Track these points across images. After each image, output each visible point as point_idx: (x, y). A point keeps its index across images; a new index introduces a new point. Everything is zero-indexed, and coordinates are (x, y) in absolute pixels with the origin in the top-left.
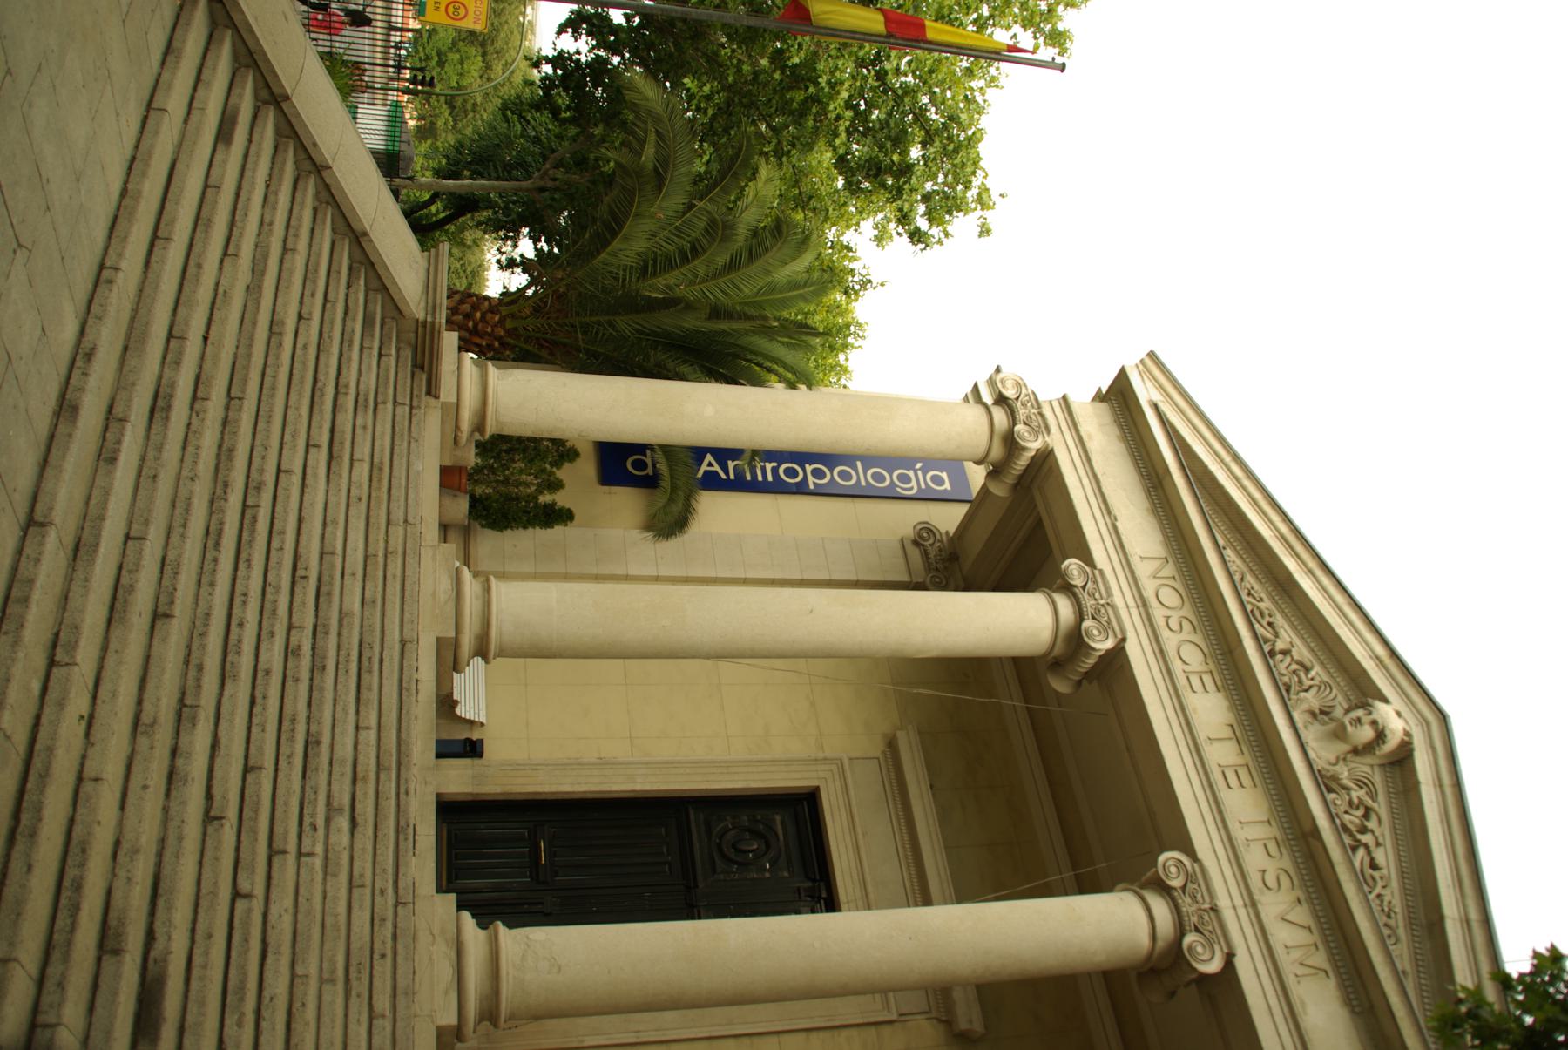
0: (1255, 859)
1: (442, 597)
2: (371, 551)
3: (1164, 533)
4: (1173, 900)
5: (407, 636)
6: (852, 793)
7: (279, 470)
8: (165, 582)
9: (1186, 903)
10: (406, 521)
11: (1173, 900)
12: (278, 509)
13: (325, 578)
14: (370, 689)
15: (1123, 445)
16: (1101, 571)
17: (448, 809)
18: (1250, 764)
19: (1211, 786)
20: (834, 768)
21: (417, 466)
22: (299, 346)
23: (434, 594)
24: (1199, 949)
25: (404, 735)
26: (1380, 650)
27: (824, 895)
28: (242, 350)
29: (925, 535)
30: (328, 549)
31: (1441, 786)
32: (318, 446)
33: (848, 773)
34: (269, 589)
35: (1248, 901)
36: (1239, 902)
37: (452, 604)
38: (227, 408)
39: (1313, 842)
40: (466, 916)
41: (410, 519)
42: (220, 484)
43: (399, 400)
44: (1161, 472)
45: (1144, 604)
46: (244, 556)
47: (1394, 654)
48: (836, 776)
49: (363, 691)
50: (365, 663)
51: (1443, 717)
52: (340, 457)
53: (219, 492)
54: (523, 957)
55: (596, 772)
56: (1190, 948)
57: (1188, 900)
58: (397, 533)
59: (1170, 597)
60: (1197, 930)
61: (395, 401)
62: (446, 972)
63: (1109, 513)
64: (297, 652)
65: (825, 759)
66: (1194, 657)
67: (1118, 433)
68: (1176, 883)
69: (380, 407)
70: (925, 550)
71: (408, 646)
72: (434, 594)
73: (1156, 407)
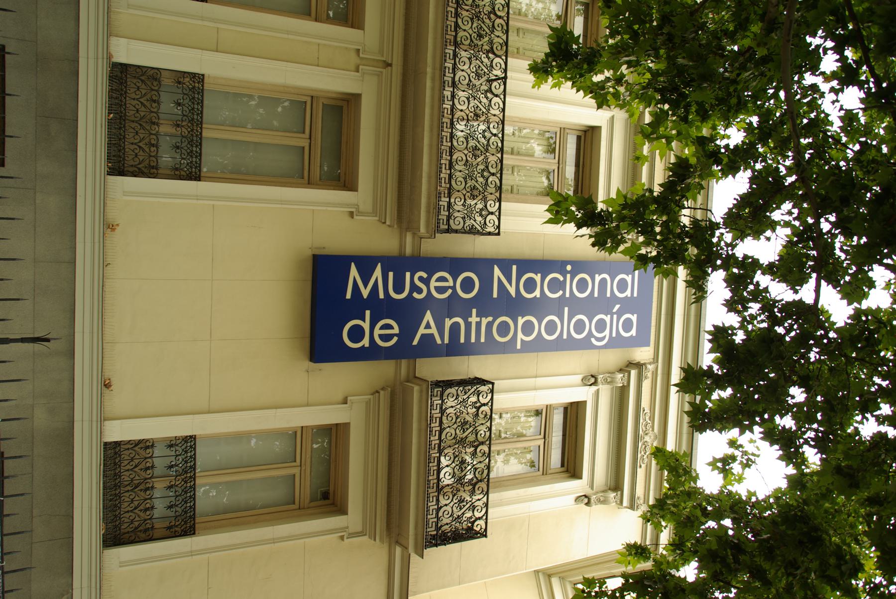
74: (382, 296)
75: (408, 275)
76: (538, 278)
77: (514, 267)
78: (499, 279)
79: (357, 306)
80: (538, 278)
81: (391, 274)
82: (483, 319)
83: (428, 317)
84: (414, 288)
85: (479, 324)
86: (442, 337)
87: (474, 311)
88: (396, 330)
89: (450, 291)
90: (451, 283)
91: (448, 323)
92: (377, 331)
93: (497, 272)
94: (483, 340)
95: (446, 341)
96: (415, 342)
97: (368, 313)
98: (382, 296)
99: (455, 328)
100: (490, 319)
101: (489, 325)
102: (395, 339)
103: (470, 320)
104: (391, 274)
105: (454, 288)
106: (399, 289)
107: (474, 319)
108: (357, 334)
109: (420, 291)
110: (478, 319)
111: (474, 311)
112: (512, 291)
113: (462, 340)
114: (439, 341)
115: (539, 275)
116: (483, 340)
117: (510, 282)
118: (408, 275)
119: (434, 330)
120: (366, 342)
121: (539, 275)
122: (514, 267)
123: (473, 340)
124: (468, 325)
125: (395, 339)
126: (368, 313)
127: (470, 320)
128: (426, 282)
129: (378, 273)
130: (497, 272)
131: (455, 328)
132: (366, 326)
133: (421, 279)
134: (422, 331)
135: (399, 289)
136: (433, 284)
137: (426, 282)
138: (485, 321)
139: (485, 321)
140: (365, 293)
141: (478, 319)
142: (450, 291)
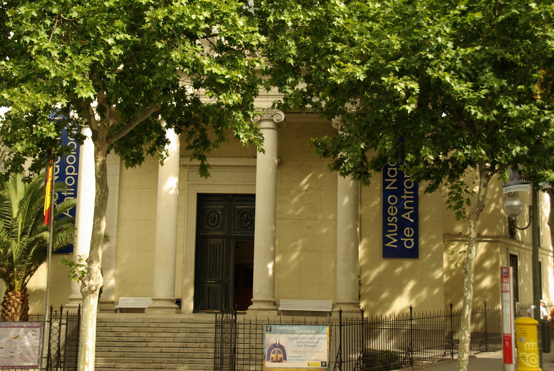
1: (163, 312)
2: (163, 331)
4: (263, 120)
5: (179, 321)
6: (200, 183)
7: (161, 352)
8: (209, 368)
9: (265, 117)
10: (143, 322)
11: (263, 120)
12: (172, 351)
13: (181, 341)
14: (203, 330)
17: (196, 310)
20: (191, 187)
21: (123, 320)
22: (120, 351)
23: (163, 314)
24: (278, 118)
25: (208, 322)
27: (231, 197)
28: (138, 362)
30: (173, 341)
32: (147, 345)
33: (193, 183)
34: (194, 352)
35: (266, 97)
36: (266, 99)
37: (165, 310)
38: (156, 363)
40: (249, 308)
41: (142, 321)
42: (178, 362)
43: (104, 325)
46: (191, 357)
48: (194, 187)
49: (203, 332)
50: (196, 331)
52: (144, 339)
53: (180, 362)
54: (262, 295)
55: (188, 264)
56: (277, 120)
57: (264, 116)
58: (151, 325)
60: (272, 116)
61: (104, 327)
62: (265, 313)
64: (206, 346)
65: (188, 189)
69: (113, 330)
71: (183, 321)
72: (163, 314)
74: (396, 234)
75: (389, 224)
76: (390, 169)
77: (386, 180)
78: (390, 187)
79: (400, 243)
80: (390, 169)
81: (389, 231)
82: (405, 193)
83: (403, 216)
84: (393, 222)
85: (407, 195)
86: (411, 210)
87: (402, 197)
88: (408, 228)
89: (395, 207)
90: (392, 207)
91: (406, 208)
92: (408, 236)
93: (388, 188)
94: (412, 193)
95: (413, 208)
96: (412, 221)
97: (402, 239)
98: (396, 234)
99: (408, 205)
100: (405, 190)
101: (408, 190)
102: (411, 229)
103: (405, 199)
104: (389, 231)
105: (394, 206)
106: (393, 228)
107: (405, 197)
108: (409, 243)
109: (395, 219)
110: (405, 195)
111: (402, 197)
112: (394, 180)
113: (412, 201)
114: (412, 211)
115: (388, 169)
116: (412, 193)
117: (391, 182)
118: (389, 224)
119: (408, 213)
120: (412, 240)
121: (388, 169)
122: (386, 180)
123: (413, 197)
124: (407, 199)
125: (411, 229)
126: (402, 239)
127: (405, 199)
128: (391, 217)
129: (388, 236)
130: (388, 188)
131: (408, 205)
132: (406, 240)
133: (390, 219)
134: (408, 218)
135: (393, 228)
136: (392, 214)
137: (391, 217)
138: (406, 192)
139: (406, 192)
140: (396, 240)
141: (405, 195)
142: (395, 207)
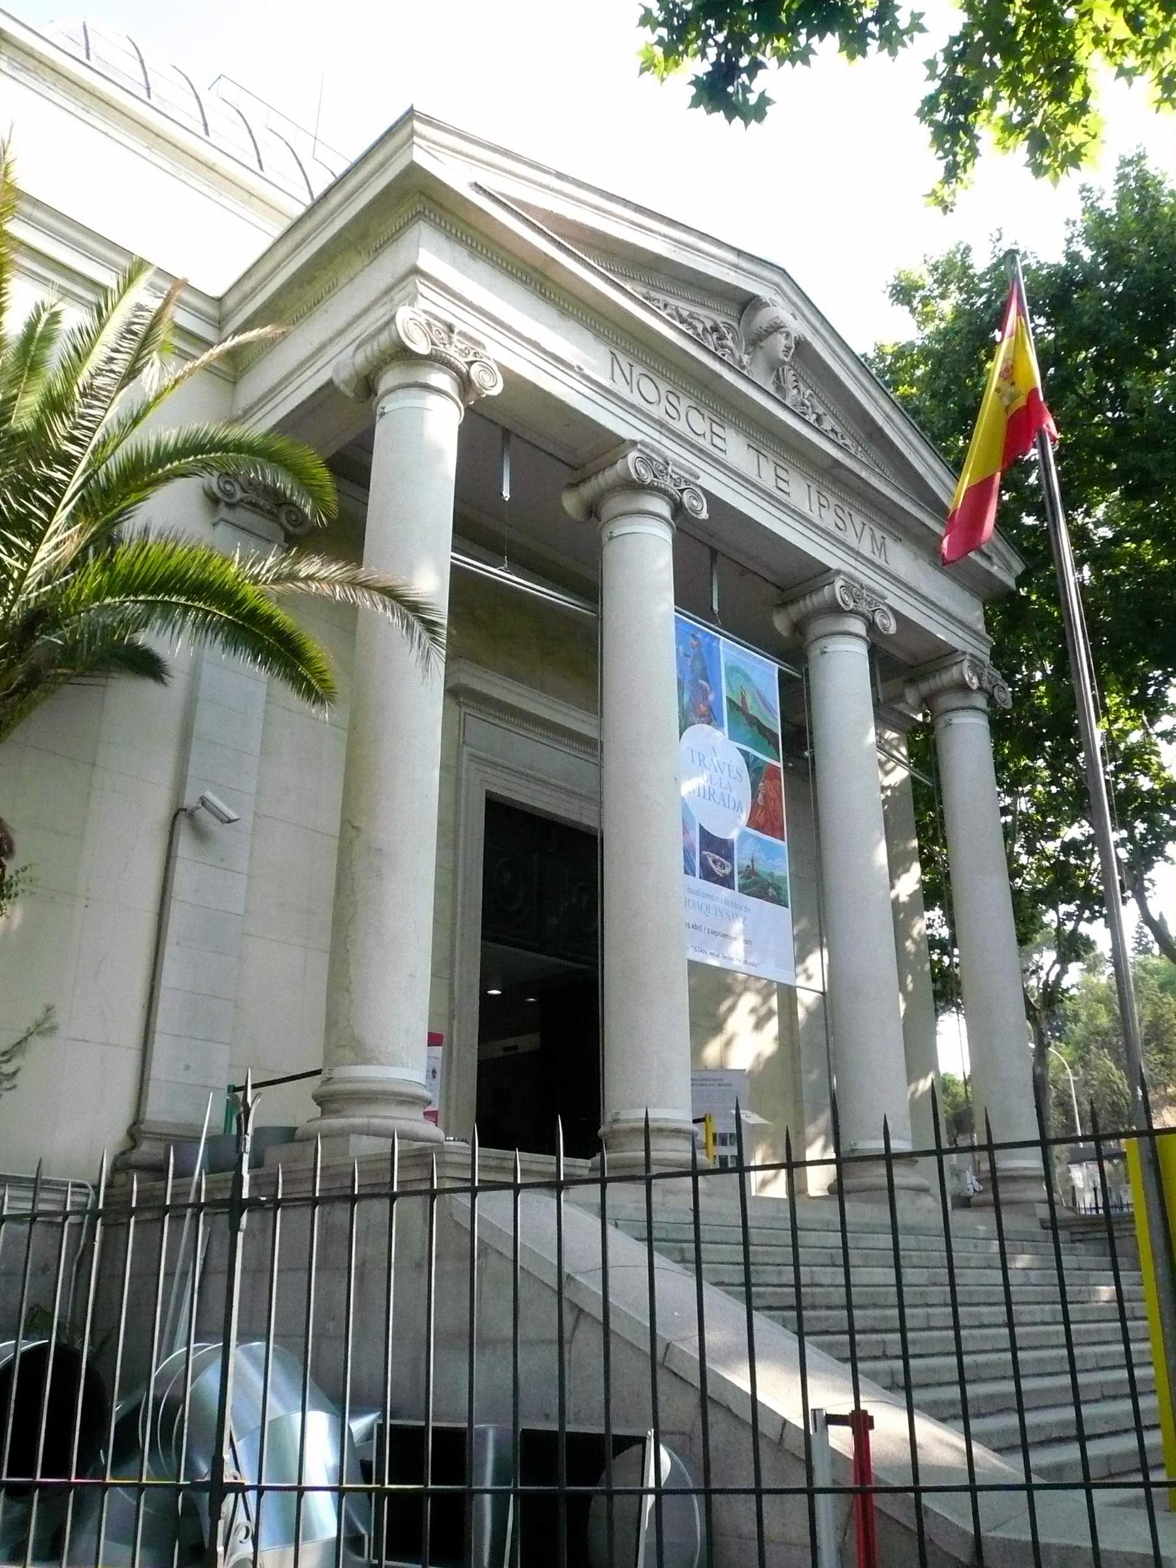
0: (828, 520)
3: (589, 327)
15: (481, 263)
16: (642, 443)
18: (778, 462)
19: (794, 511)
26: (731, 257)
29: (228, 487)
31: (817, 331)
39: (836, 471)
44: (538, 264)
45: (662, 424)
47: (740, 253)
51: (784, 270)
59: (647, 387)
63: (570, 367)
66: (700, 424)
67: (465, 252)
68: (852, 605)
70: (250, 503)
73: (478, 187)
